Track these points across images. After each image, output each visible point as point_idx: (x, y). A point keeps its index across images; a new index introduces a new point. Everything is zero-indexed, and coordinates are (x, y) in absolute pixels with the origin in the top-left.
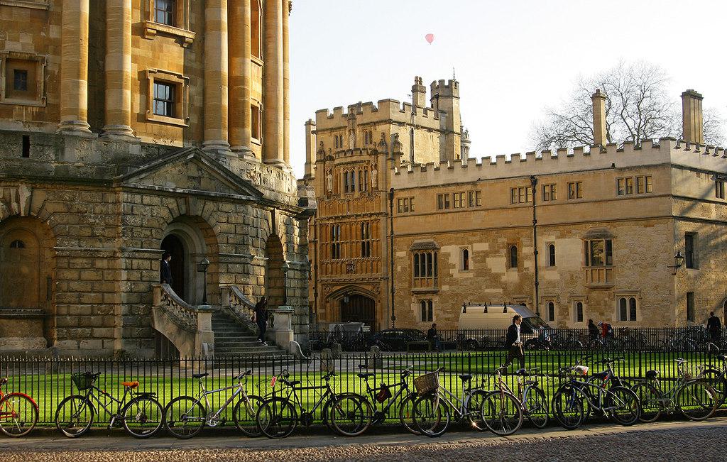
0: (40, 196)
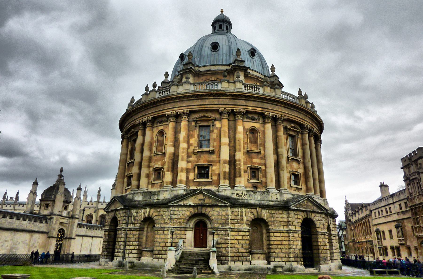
0: (152, 210)
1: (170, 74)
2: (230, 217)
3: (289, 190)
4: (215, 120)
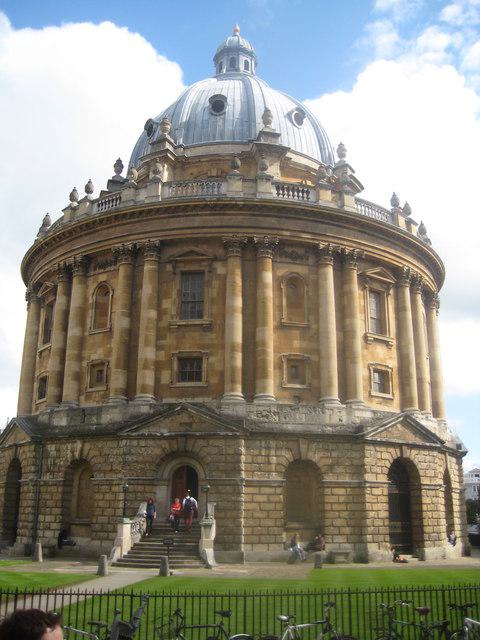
0: (87, 446)
1: (126, 164)
2: (243, 458)
3: (366, 403)
4: (216, 259)
